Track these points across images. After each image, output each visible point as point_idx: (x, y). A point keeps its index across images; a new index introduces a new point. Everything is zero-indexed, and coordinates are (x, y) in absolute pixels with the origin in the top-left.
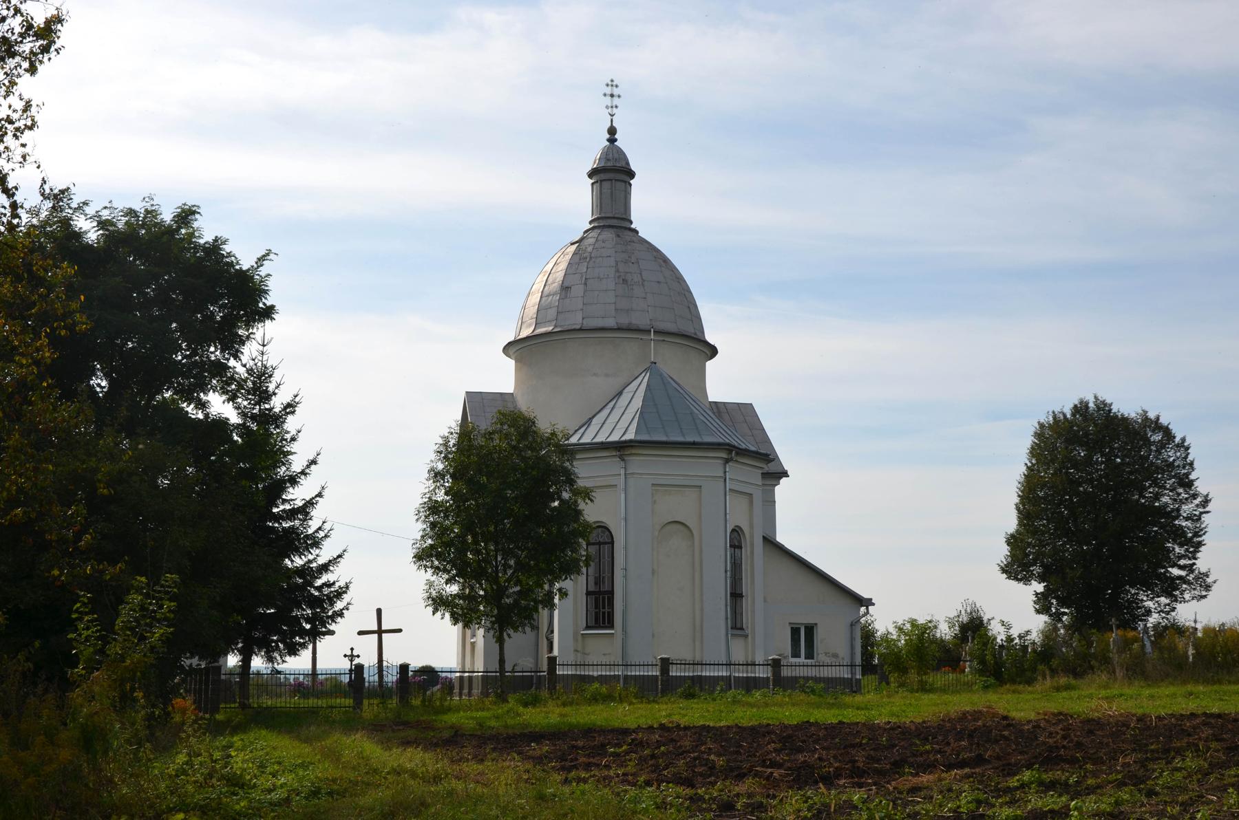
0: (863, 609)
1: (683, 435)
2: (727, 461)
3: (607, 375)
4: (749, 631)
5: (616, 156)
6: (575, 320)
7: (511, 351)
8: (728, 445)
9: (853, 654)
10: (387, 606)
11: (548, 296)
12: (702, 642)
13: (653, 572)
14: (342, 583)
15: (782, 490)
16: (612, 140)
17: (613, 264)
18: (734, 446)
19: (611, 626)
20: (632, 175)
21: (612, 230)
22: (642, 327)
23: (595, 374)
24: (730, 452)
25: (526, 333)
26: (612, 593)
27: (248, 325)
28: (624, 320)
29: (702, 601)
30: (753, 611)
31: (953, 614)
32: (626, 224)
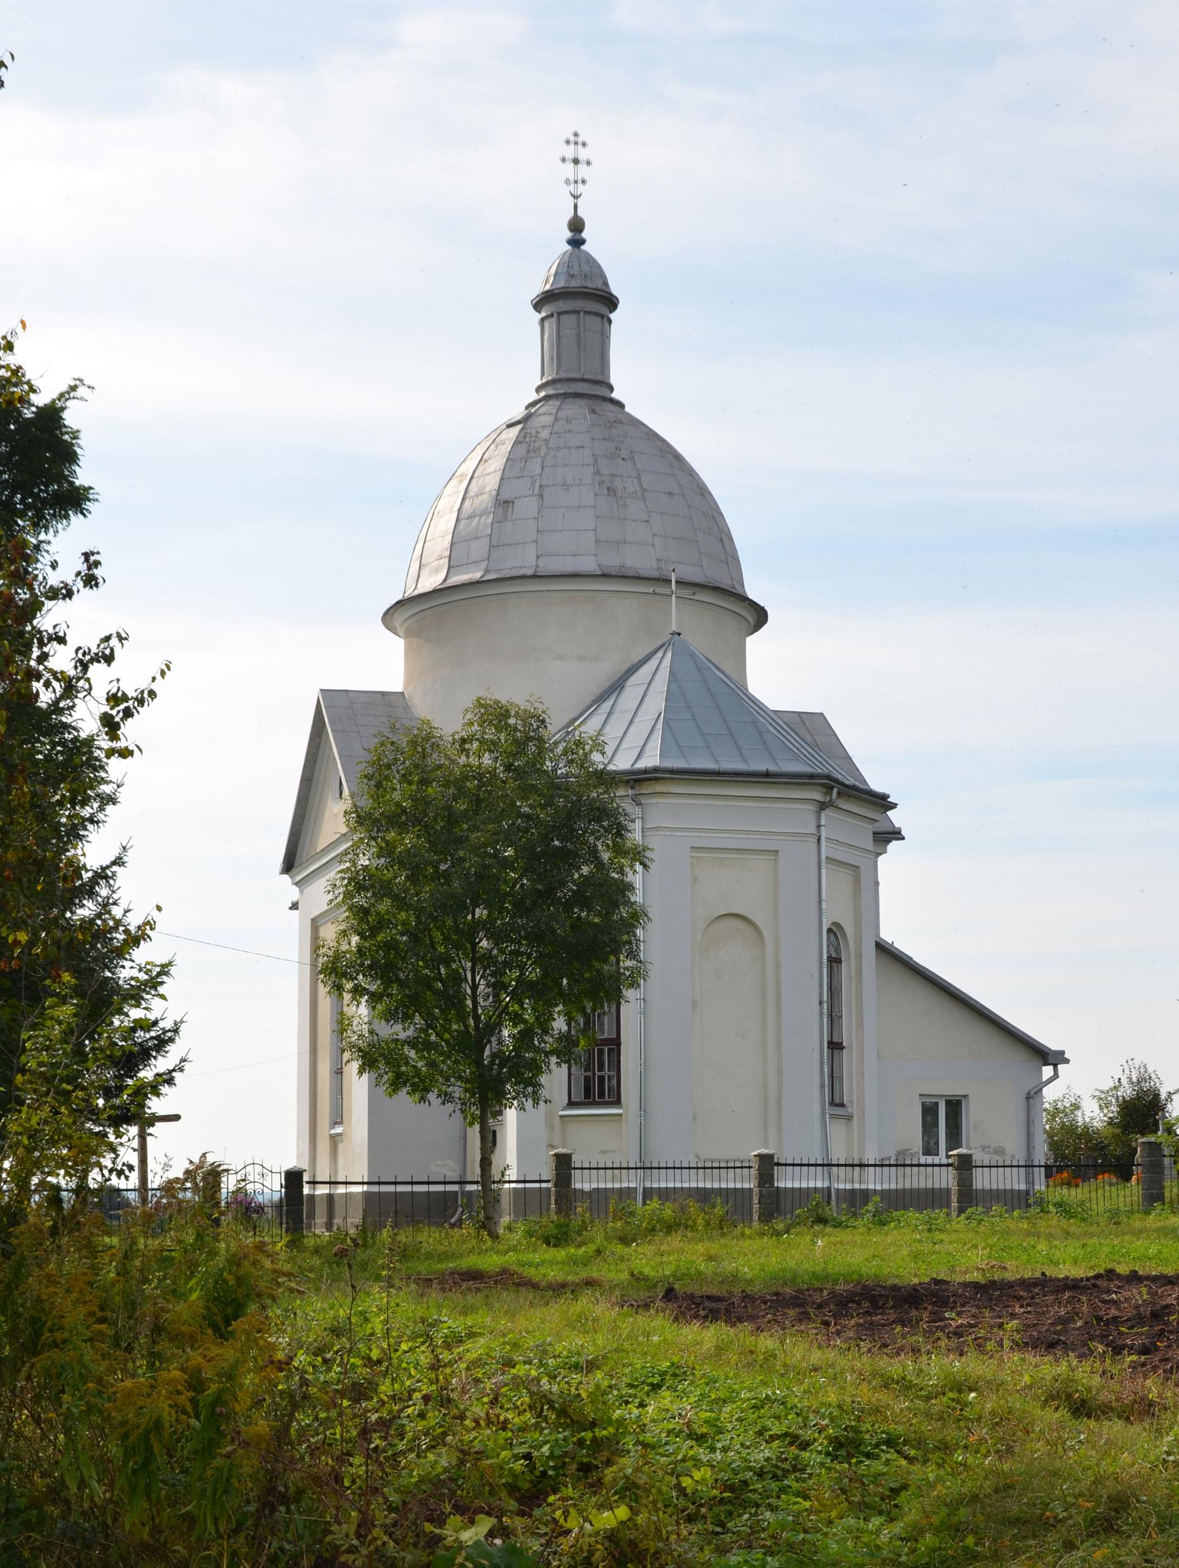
0: (1047, 1071)
1: (745, 761)
2: (822, 806)
3: (581, 659)
4: (853, 1109)
5: (586, 269)
6: (524, 560)
7: (399, 618)
8: (828, 777)
9: (1030, 1148)
10: (244, 1063)
11: (471, 517)
12: (779, 1128)
13: (694, 1004)
14: (166, 1024)
15: (891, 865)
16: (576, 242)
17: (591, 460)
18: (837, 781)
19: (617, 1102)
20: (611, 303)
21: (583, 402)
22: (643, 573)
23: (560, 657)
24: (829, 789)
25: (430, 582)
26: (616, 1042)
27: (39, 523)
28: (611, 561)
29: (780, 1056)
30: (861, 1074)
31: (1108, 1085)
32: (601, 391)
